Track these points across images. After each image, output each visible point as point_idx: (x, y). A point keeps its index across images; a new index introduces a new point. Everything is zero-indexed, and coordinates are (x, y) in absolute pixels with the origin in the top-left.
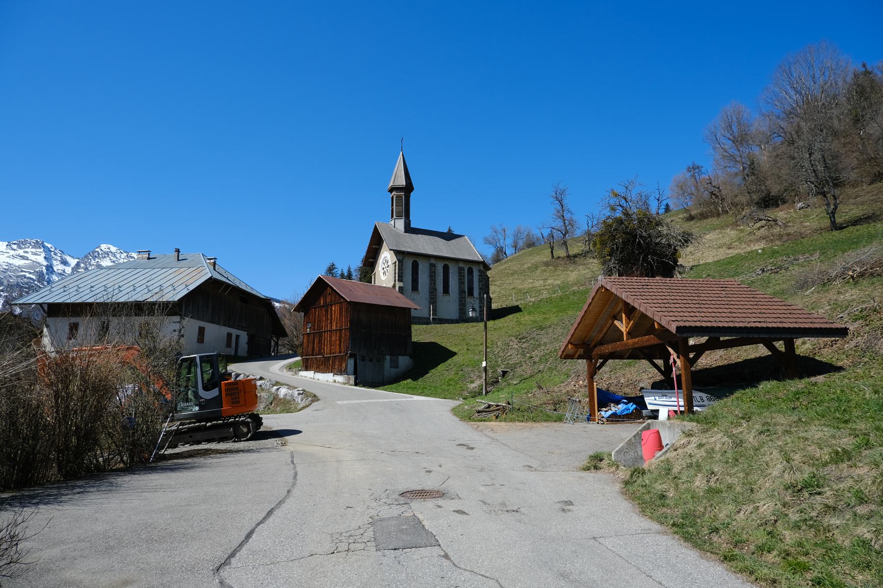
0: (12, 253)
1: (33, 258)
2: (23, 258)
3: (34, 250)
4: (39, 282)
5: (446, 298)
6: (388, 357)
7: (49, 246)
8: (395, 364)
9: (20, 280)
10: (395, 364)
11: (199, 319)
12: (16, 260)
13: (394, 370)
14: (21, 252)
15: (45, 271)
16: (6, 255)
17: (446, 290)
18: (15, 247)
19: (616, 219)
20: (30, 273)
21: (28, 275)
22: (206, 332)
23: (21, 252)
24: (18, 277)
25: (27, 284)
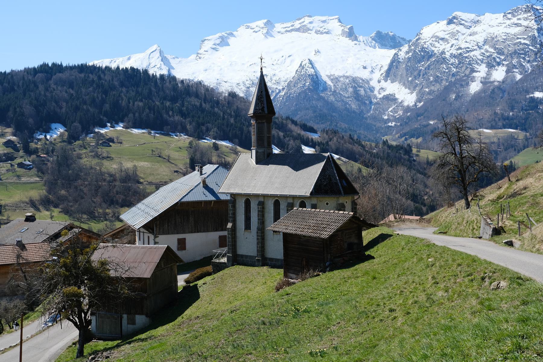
0: (508, 22)
1: (525, 23)
2: (517, 25)
3: (525, 16)
4: (532, 46)
5: (247, 234)
6: (125, 316)
7: (538, 8)
8: (132, 321)
9: (517, 48)
10: (132, 321)
11: (178, 233)
12: (512, 28)
13: (131, 327)
14: (515, 20)
15: (536, 34)
16: (504, 25)
17: (248, 227)
18: (509, 16)
19: (60, 236)
20: (525, 39)
21: (523, 41)
22: (187, 241)
23: (515, 20)
24: (515, 44)
25: (523, 50)
